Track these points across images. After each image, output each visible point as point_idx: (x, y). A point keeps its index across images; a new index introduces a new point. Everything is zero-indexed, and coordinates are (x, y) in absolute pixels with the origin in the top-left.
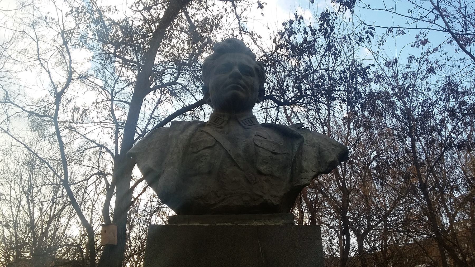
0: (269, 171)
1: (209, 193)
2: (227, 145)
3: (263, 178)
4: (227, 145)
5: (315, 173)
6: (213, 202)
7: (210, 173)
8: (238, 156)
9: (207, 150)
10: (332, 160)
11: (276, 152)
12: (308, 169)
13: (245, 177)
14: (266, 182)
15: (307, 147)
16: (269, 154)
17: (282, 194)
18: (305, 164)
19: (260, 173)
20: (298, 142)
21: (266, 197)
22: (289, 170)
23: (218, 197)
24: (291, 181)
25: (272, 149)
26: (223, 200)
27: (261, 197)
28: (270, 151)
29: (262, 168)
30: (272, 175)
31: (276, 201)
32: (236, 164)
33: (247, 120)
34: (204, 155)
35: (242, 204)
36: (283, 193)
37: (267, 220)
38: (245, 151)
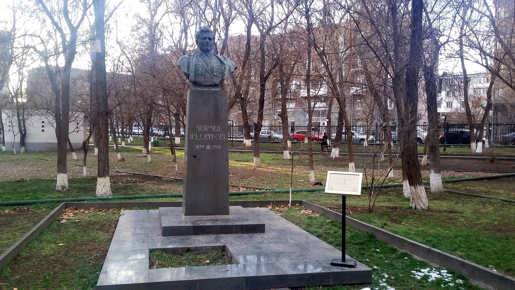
2: (206, 66)
4: (206, 66)
7: (202, 75)
8: (209, 70)
15: (227, 67)
16: (216, 70)
17: (219, 81)
18: (225, 72)
20: (224, 66)
22: (221, 74)
24: (222, 77)
25: (217, 68)
29: (215, 74)
30: (217, 76)
31: (218, 83)
32: (208, 73)
38: (211, 69)
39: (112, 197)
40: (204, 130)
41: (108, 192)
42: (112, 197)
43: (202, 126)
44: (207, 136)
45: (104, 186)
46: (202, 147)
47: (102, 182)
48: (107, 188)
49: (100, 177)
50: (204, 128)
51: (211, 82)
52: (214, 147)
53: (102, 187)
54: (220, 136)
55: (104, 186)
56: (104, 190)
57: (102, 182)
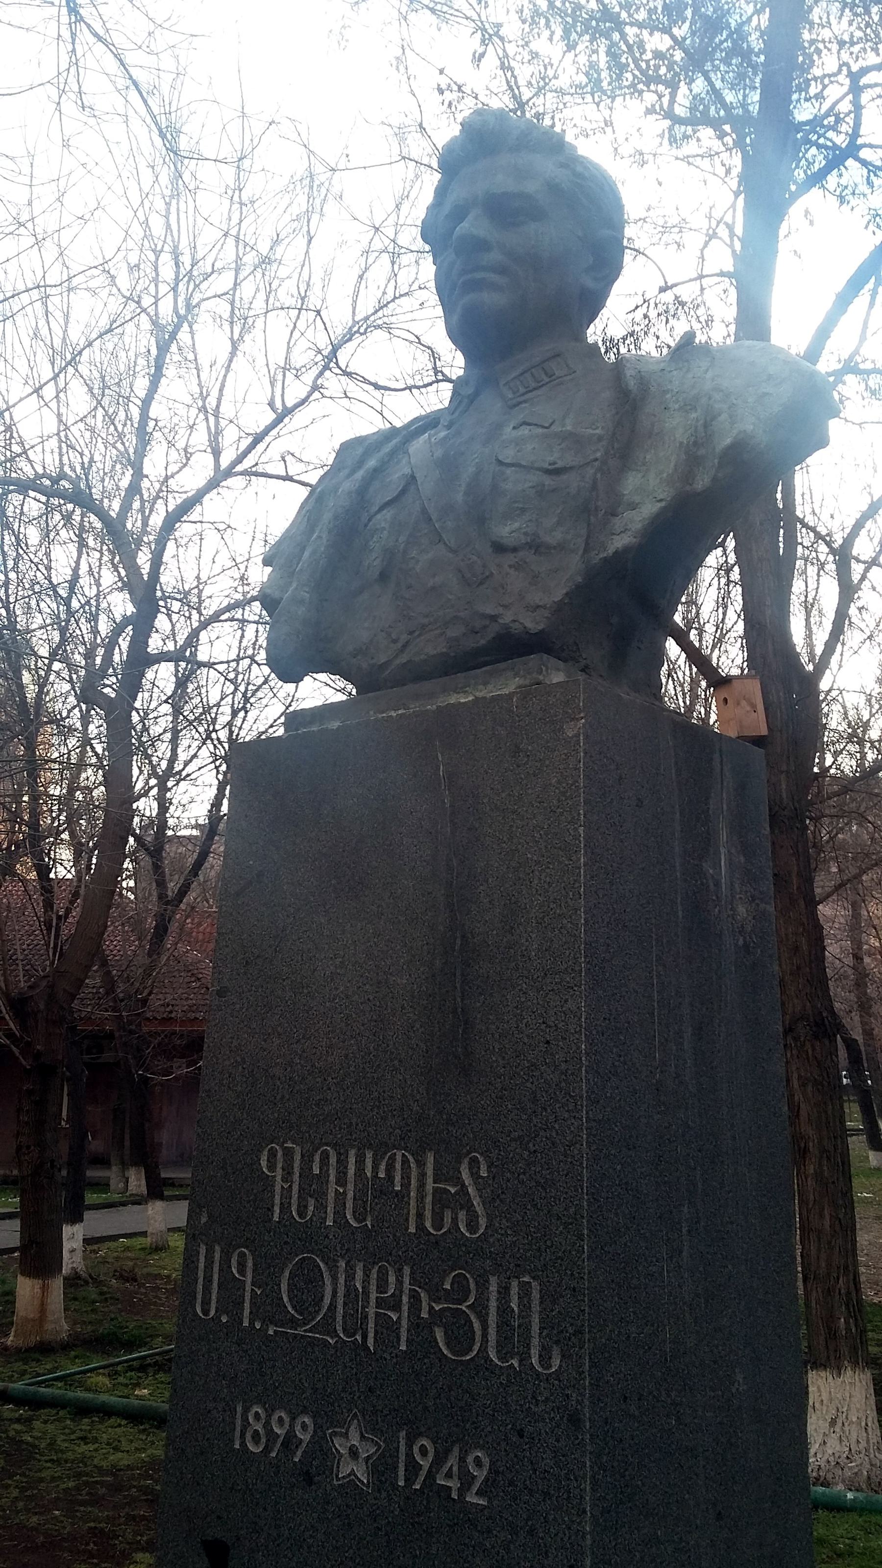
0: (526, 534)
1: (375, 635)
3: (510, 559)
5: (663, 504)
6: (383, 659)
9: (385, 511)
10: (728, 441)
11: (560, 464)
12: (637, 499)
13: (460, 571)
14: (516, 569)
17: (558, 594)
19: (500, 548)
21: (507, 618)
23: (395, 641)
26: (405, 646)
27: (494, 618)
28: (539, 469)
30: (536, 546)
33: (528, 375)
34: (377, 529)
35: (444, 650)
36: (564, 591)
37: (481, 687)
39: (860, 1495)
40: (321, 1207)
41: (858, 1459)
42: (860, 1496)
43: (307, 1160)
44: (350, 1290)
45: (833, 1423)
46: (290, 1443)
47: (825, 1396)
48: (854, 1433)
49: (818, 1365)
50: (323, 1177)
51: (454, 632)
52: (413, 1467)
53: (824, 1426)
54: (480, 1309)
55: (833, 1423)
56: (833, 1446)
57: (825, 1396)
